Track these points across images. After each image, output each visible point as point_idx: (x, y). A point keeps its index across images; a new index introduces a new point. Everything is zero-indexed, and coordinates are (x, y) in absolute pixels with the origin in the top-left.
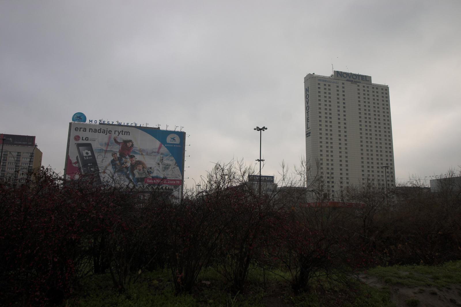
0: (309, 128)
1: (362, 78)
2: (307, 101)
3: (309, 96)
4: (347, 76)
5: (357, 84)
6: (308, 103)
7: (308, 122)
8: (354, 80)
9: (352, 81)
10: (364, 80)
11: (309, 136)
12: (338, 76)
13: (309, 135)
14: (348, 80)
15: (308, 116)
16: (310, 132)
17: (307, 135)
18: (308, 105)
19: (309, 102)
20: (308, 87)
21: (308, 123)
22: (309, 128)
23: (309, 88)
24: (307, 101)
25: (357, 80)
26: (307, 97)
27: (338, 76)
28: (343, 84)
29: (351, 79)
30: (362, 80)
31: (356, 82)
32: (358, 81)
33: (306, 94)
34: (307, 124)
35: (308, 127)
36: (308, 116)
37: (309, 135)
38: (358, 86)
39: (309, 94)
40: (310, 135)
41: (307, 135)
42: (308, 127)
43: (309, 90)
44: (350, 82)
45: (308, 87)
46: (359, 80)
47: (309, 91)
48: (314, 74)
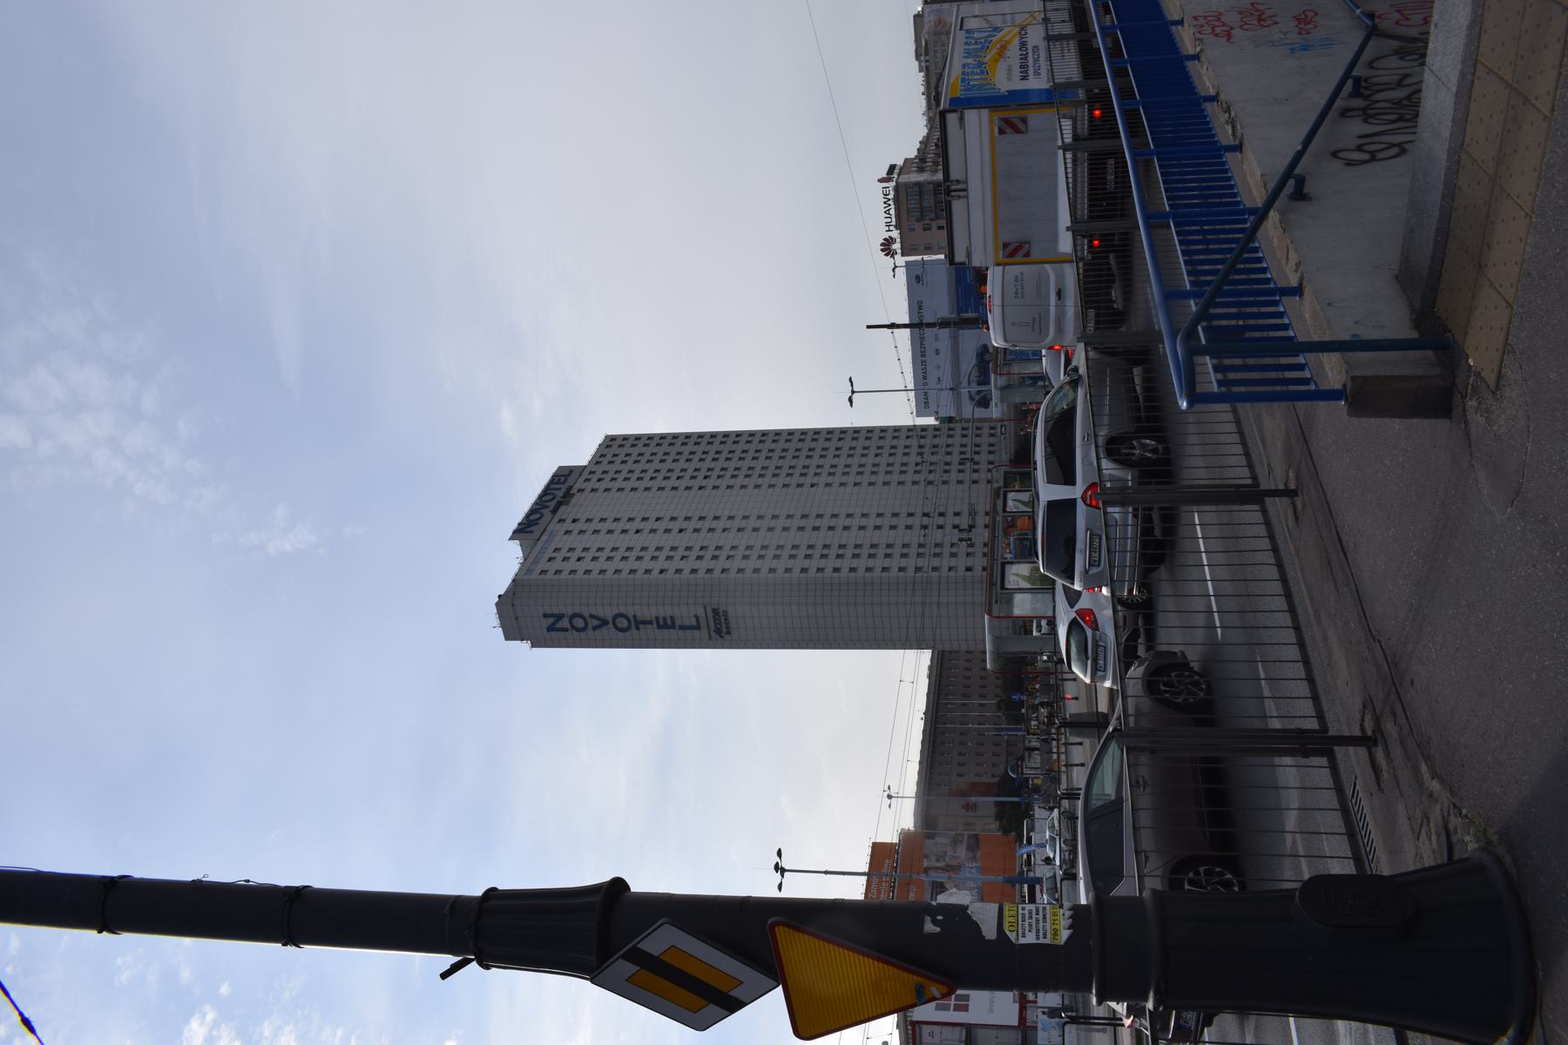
0: (697, 617)
1: (558, 483)
2: (596, 623)
3: (578, 610)
4: (541, 513)
5: (574, 494)
6: (604, 622)
7: (673, 626)
8: (558, 499)
9: (559, 505)
10: (566, 480)
11: (726, 619)
12: (532, 532)
13: (723, 618)
14: (554, 512)
15: (650, 623)
16: (715, 611)
17: (725, 630)
18: (610, 620)
19: (601, 614)
20: (545, 616)
21: (678, 623)
22: (697, 617)
23: (548, 611)
24: (595, 628)
25: (560, 494)
26: (579, 623)
27: (532, 532)
28: (561, 521)
29: (552, 505)
30: (564, 482)
31: (568, 495)
32: (564, 490)
33: (567, 630)
34: (681, 628)
35: (694, 622)
36: (650, 623)
37: (723, 618)
38: (580, 490)
39: (570, 611)
40: (725, 612)
41: (725, 630)
42: (694, 622)
43: (556, 611)
44: (562, 508)
45: (545, 616)
46: (560, 489)
47: (562, 610)
48: (500, 596)
